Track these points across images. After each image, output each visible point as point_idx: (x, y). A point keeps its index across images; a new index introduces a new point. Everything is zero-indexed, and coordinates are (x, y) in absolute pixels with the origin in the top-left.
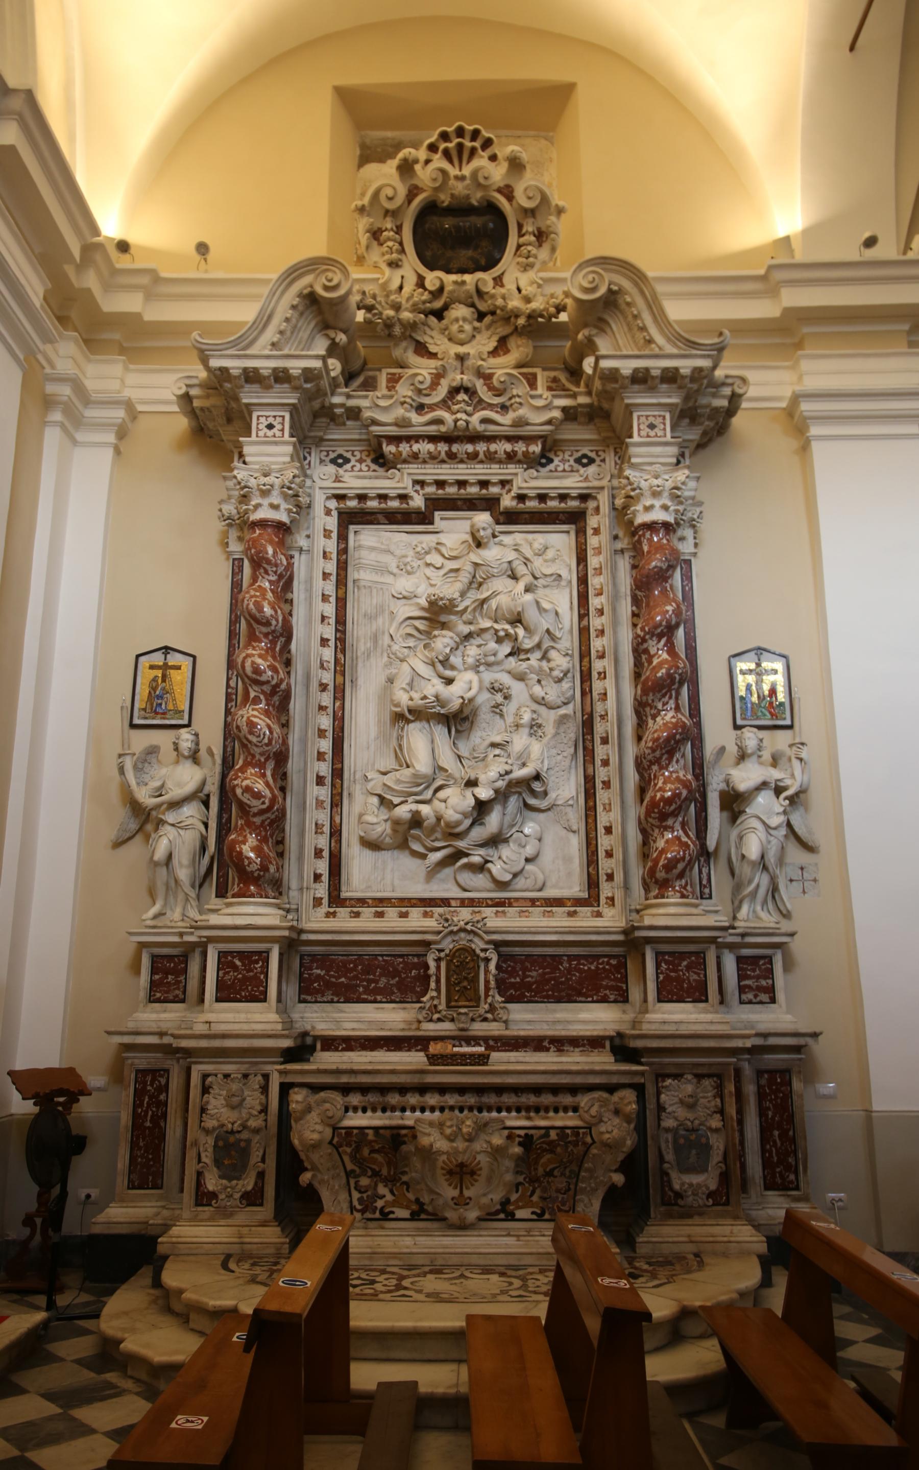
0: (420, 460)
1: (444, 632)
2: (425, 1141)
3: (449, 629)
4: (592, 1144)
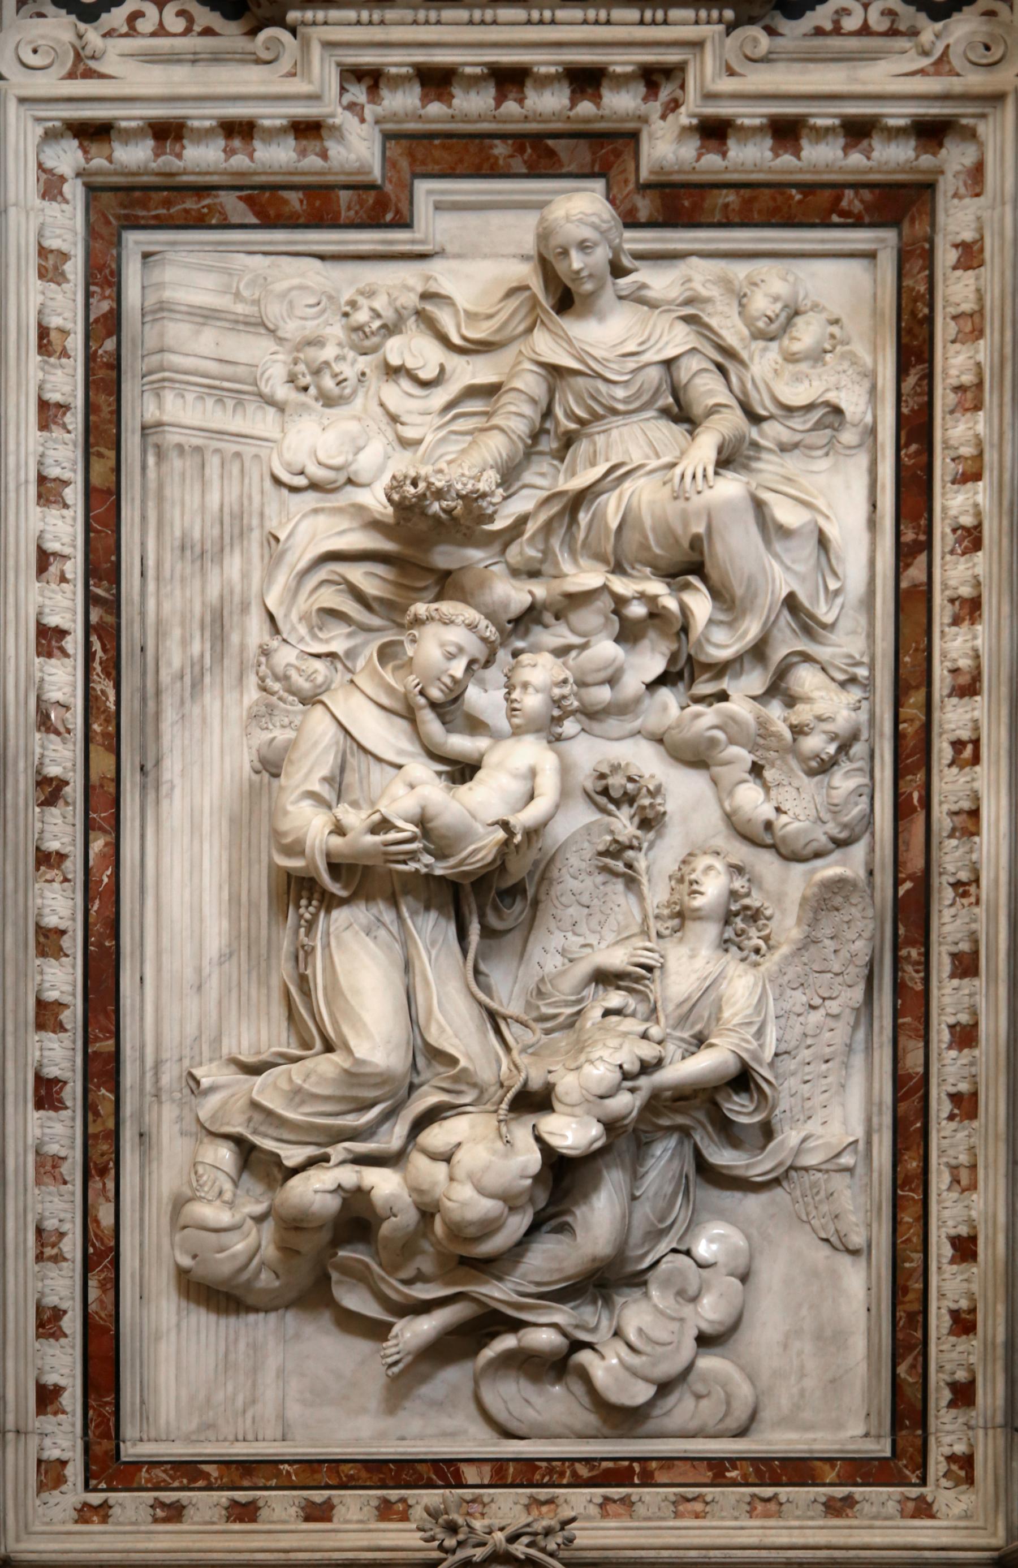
1: (447, 607)
3: (464, 596)
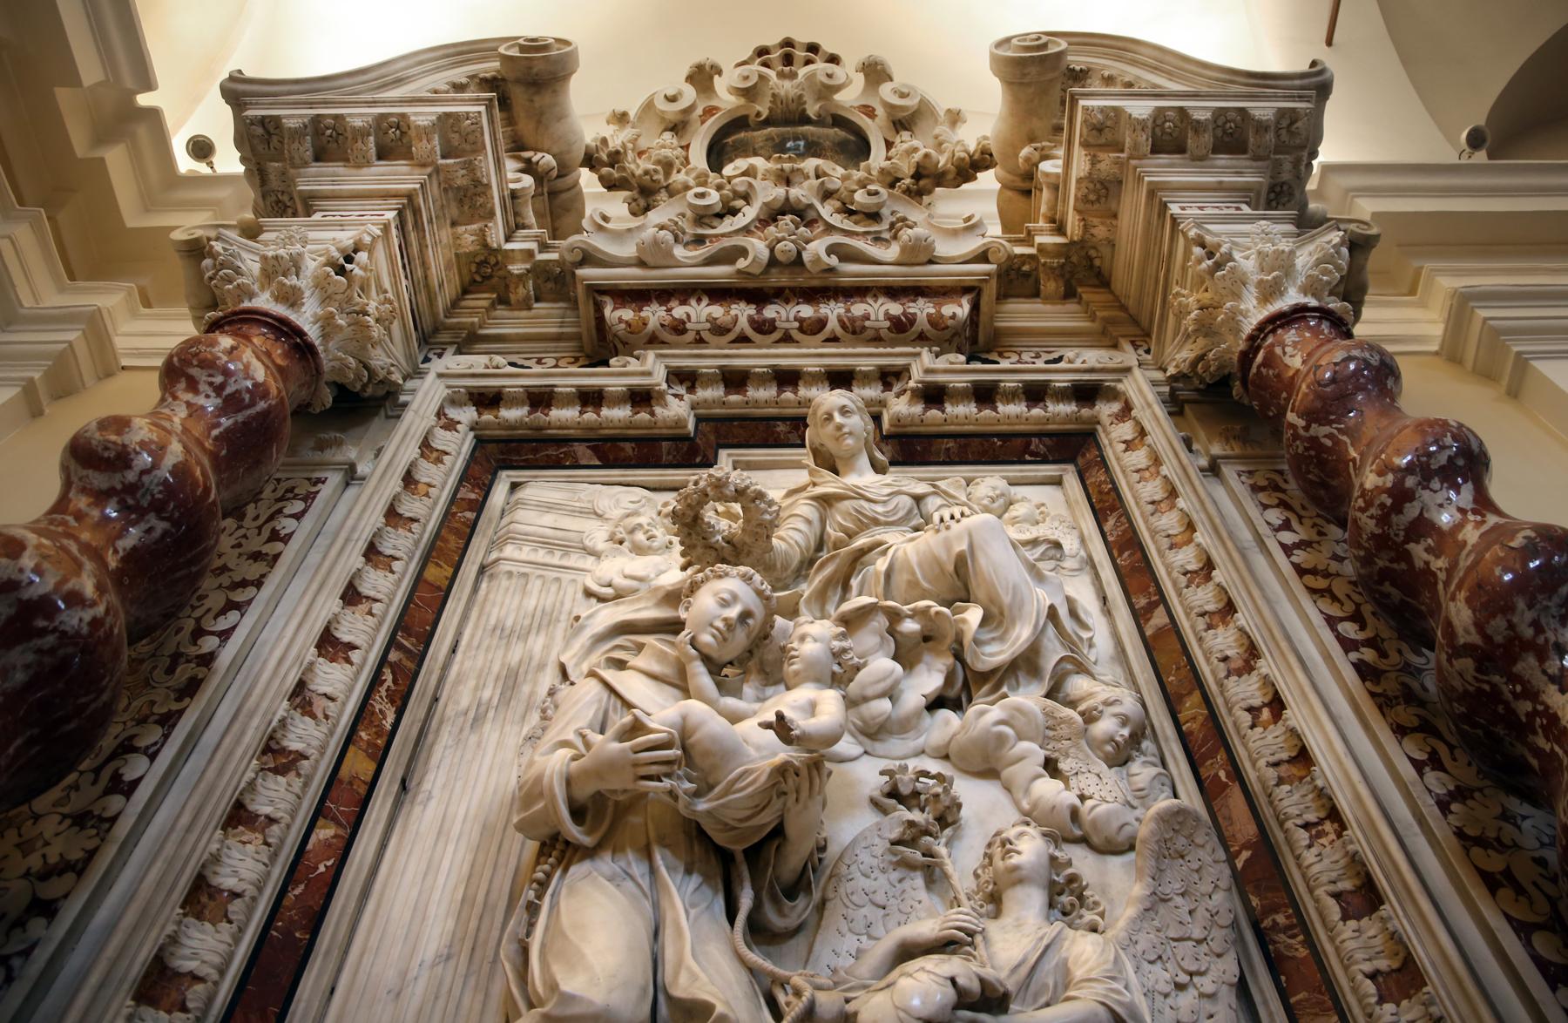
0: (690, 336)
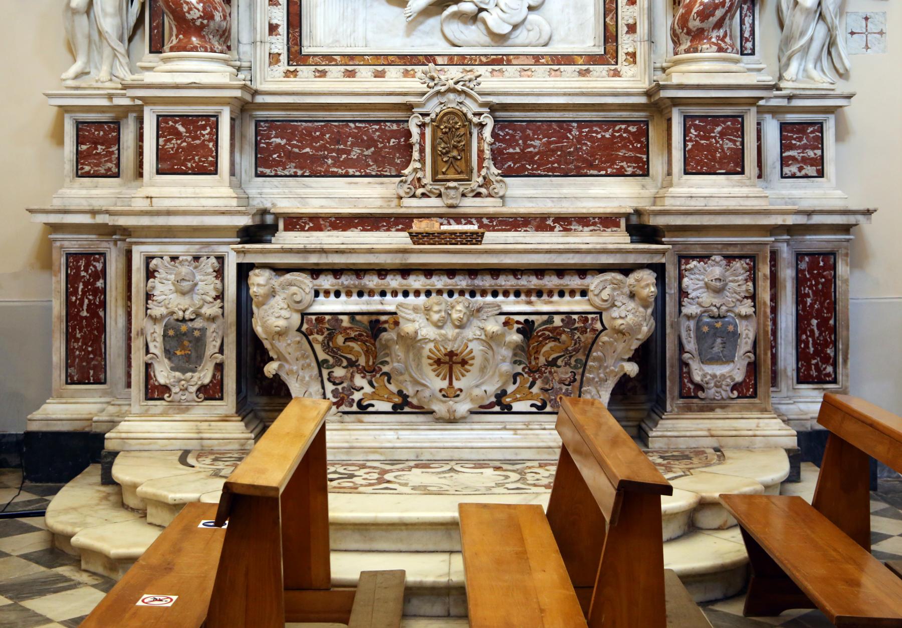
2: (408, 328)
4: (602, 331)
